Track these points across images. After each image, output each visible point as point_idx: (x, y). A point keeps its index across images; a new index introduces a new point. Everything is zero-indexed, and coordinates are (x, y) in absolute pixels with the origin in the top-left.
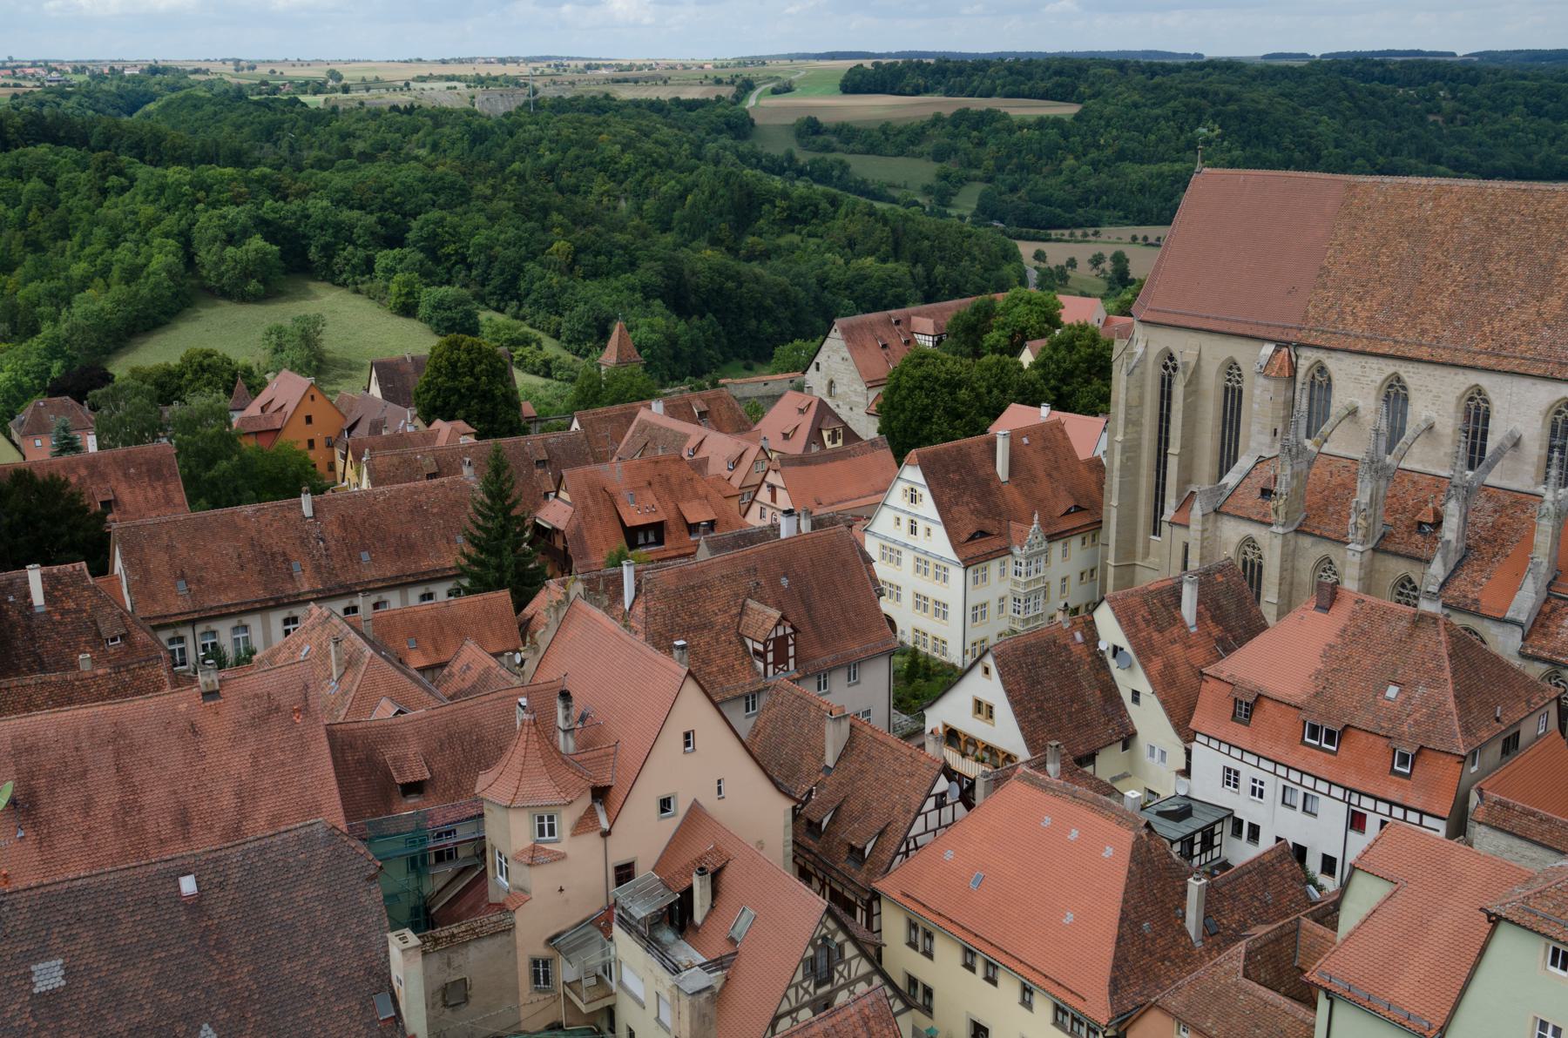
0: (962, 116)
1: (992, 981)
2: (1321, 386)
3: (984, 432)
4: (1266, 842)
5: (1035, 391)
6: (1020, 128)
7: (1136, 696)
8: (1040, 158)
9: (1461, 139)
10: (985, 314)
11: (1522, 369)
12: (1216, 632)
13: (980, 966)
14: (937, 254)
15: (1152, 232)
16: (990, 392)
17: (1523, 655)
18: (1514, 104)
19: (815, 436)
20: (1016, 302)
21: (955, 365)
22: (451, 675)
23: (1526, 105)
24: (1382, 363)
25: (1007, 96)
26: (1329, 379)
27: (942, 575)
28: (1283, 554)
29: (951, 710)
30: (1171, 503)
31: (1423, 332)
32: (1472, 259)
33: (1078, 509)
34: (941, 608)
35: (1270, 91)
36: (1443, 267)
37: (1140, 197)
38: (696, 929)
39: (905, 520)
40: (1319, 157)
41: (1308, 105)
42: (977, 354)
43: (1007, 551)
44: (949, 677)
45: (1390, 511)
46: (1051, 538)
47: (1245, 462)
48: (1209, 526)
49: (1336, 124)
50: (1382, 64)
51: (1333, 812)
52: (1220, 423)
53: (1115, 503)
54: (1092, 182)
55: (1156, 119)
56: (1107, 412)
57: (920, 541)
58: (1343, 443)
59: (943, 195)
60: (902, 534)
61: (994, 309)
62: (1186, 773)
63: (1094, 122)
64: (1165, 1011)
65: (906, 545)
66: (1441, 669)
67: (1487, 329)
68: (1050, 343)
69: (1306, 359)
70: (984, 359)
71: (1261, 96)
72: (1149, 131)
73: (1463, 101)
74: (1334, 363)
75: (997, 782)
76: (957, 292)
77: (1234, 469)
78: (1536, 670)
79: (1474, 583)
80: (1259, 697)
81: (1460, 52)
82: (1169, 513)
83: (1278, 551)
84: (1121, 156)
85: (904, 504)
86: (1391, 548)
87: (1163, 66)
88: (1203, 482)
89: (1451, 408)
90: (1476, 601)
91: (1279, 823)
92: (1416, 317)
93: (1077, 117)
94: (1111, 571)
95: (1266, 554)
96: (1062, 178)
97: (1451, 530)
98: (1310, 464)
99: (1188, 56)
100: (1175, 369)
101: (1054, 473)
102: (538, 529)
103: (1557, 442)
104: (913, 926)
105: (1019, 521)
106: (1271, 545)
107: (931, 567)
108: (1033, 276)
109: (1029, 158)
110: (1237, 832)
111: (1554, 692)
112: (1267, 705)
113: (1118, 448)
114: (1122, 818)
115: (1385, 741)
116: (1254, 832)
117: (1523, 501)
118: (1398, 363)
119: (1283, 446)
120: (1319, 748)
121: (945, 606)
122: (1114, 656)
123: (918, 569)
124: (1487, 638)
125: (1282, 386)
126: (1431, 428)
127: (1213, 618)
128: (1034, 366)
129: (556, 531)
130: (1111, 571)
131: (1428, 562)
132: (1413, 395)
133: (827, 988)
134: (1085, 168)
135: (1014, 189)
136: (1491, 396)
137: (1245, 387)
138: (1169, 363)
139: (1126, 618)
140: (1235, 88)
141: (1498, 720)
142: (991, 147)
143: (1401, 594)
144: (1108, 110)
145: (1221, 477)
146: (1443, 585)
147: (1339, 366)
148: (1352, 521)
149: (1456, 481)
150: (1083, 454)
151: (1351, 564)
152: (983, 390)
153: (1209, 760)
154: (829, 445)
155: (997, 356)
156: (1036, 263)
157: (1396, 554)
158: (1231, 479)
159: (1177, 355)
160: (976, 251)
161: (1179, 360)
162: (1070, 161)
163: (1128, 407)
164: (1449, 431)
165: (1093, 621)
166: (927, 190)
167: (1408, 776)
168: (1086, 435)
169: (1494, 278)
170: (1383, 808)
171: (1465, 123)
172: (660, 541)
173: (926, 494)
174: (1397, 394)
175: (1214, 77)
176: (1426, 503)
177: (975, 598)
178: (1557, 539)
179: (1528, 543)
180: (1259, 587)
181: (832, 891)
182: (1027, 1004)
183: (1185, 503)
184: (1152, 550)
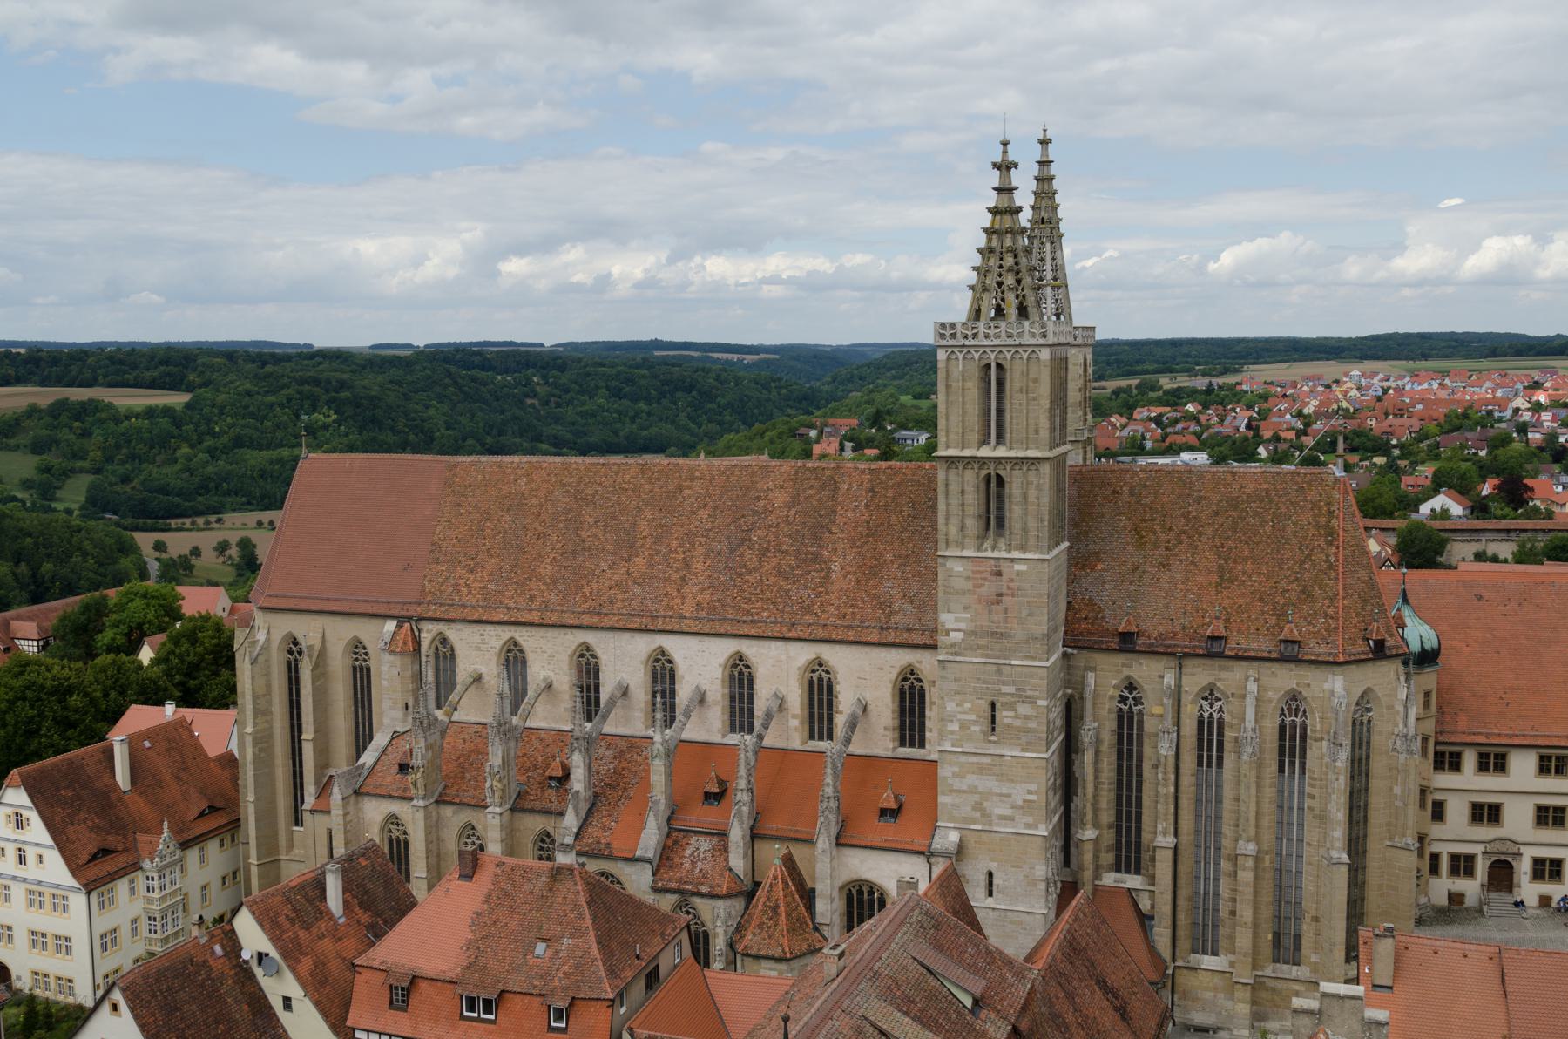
0: (61, 406)
2: (445, 657)
3: (103, 738)
5: (157, 690)
6: (128, 418)
7: (287, 1003)
8: (152, 447)
9: (557, 420)
10: (97, 612)
11: (621, 625)
12: (366, 918)
14: (43, 551)
15: (266, 516)
16: (106, 695)
17: (655, 889)
18: (597, 388)
20: (131, 596)
21: (62, 670)
23: (608, 388)
24: (499, 628)
25: (110, 385)
26: (452, 649)
27: (60, 904)
28: (426, 827)
30: (310, 790)
31: (532, 598)
32: (566, 527)
33: (213, 809)
34: (63, 942)
35: (380, 378)
36: (541, 536)
37: (261, 482)
39: (11, 850)
40: (432, 439)
41: (417, 391)
42: (91, 655)
43: (136, 867)
45: (523, 770)
46: (185, 845)
47: (380, 739)
48: (351, 808)
49: (445, 408)
50: (479, 353)
52: (352, 702)
53: (251, 798)
54: (210, 469)
55: (271, 406)
56: (235, 703)
57: (31, 871)
58: (472, 710)
59: (46, 488)
61: (106, 606)
63: (207, 410)
65: (14, 878)
66: (581, 917)
67: (587, 590)
68: (170, 638)
69: (428, 632)
70: (98, 661)
71: (371, 383)
72: (265, 417)
73: (554, 385)
74: (455, 634)
76: (69, 590)
77: (370, 748)
78: (667, 902)
79: (604, 828)
80: (414, 979)
81: (548, 343)
82: (310, 800)
83: (422, 824)
84: (238, 442)
86: (527, 805)
87: (273, 355)
88: (340, 766)
89: (565, 667)
90: (608, 845)
92: (524, 584)
93: (188, 406)
94: (254, 870)
95: (410, 830)
96: (178, 467)
97: (578, 782)
98: (443, 734)
99: (298, 346)
100: (300, 653)
101: (182, 775)
103: (659, 688)
105: (147, 831)
106: (414, 818)
107: (47, 899)
108: (154, 567)
109: (141, 448)
111: (684, 918)
112: (423, 985)
113: (249, 739)
115: (539, 999)
117: (635, 744)
118: (513, 628)
119: (415, 719)
120: (479, 1020)
121: (67, 939)
122: (260, 963)
123: (31, 903)
124: (622, 879)
125: (408, 660)
126: (549, 686)
127: (361, 905)
128: (154, 662)
130: (254, 870)
131: (561, 814)
132: (530, 657)
134: (201, 455)
135: (125, 480)
136: (599, 652)
137: (372, 664)
138: (293, 647)
139: (267, 921)
140: (345, 376)
141: (638, 957)
142: (97, 437)
143: (541, 849)
144: (221, 398)
145: (358, 757)
146: (577, 835)
147: (459, 636)
148: (488, 785)
149: (577, 734)
150: (213, 750)
151: (491, 824)
152: (98, 694)
155: (113, 655)
156: (157, 554)
157: (532, 811)
158: (368, 758)
159: (300, 639)
160: (87, 545)
161: (304, 644)
162: (185, 449)
163: (255, 697)
164: (566, 687)
165: (233, 930)
166: (27, 484)
167: (564, 1031)
168: (215, 730)
169: (587, 544)
171: (558, 405)
173: (34, 817)
174: (516, 657)
175: (325, 366)
176: (554, 757)
177: (103, 924)
178: (670, 775)
179: (646, 785)
180: (407, 864)
183: (324, 790)
184: (296, 843)
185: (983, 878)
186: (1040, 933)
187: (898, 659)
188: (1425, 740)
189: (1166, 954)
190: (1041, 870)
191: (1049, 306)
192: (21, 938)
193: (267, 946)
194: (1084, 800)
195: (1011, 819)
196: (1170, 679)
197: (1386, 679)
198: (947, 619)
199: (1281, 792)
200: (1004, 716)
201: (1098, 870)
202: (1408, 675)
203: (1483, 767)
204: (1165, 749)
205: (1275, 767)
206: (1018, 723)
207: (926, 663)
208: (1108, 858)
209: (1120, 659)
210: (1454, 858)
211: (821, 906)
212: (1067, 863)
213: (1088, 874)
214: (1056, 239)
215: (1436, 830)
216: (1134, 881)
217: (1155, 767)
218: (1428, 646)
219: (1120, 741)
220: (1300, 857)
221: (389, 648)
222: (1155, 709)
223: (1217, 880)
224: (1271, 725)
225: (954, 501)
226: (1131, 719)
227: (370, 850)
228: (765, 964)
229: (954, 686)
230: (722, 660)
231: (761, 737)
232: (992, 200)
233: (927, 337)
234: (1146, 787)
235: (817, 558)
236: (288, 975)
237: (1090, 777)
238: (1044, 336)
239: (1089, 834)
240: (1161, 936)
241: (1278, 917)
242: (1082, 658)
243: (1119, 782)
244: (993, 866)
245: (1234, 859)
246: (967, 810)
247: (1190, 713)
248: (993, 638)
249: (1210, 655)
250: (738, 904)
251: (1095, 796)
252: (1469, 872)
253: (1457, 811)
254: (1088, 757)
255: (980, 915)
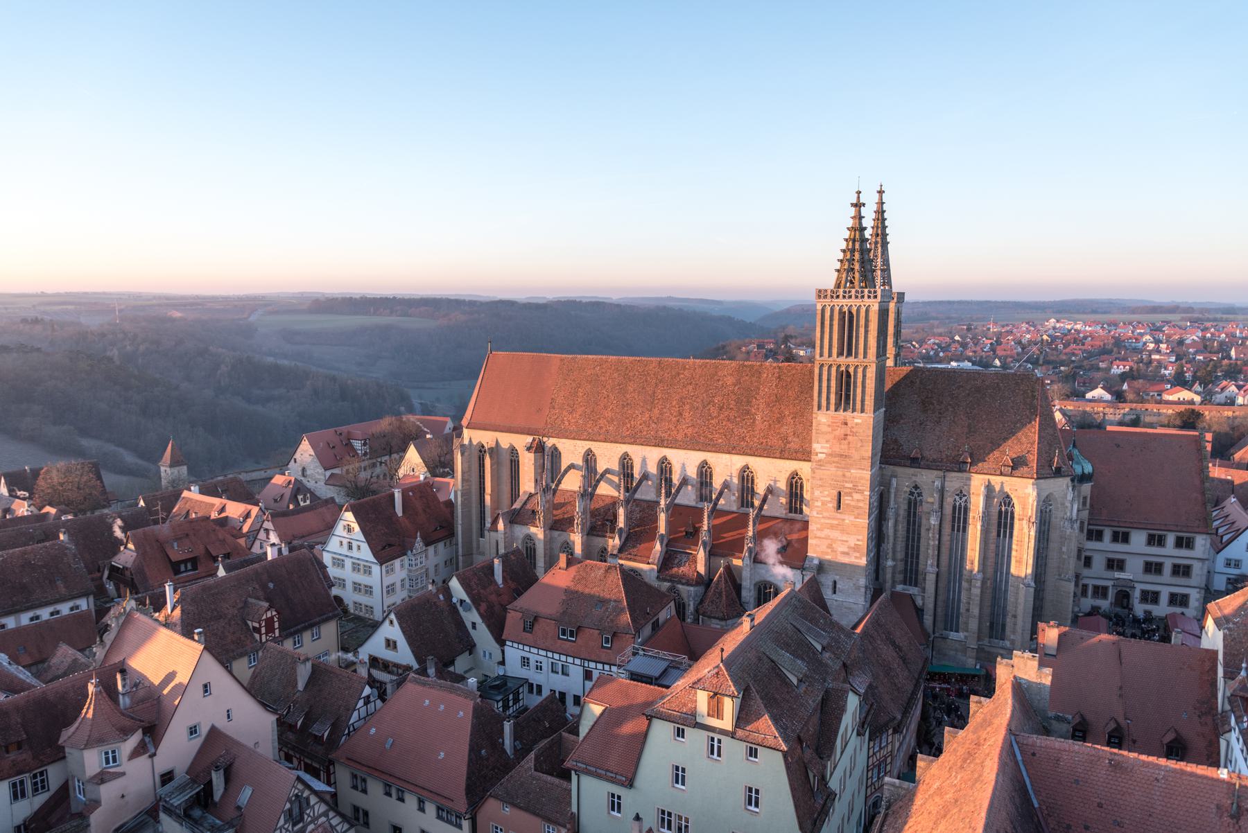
1: (401, 800)
4: (546, 693)
12: (513, 585)
13: (394, 792)
19: (294, 498)
22: (50, 667)
27: (368, 571)
29: (374, 646)
30: (488, 520)
38: (215, 804)
39: (345, 542)
44: (376, 626)
46: (427, 544)
51: (576, 671)
57: (355, 553)
60: (344, 550)
62: (503, 663)
64: (496, 797)
75: (399, 684)
82: (488, 525)
85: (345, 534)
91: (551, 682)
97: (621, 522)
102: (114, 569)
104: (354, 776)
110: (531, 691)
112: (541, 620)
114: (468, 694)
116: (539, 687)
123: (354, 569)
129: (125, 568)
130: (461, 558)
133: (301, 825)
153: (514, 653)
154: (302, 504)
158: (517, 505)
170: (600, 666)
172: (195, 568)
177: (388, 581)
181: (306, 764)
182: (422, 809)
183: (495, 522)
185: (831, 584)
186: (861, 614)
187: (789, 466)
188: (1082, 523)
189: (930, 630)
190: (862, 582)
191: (879, 281)
192: (349, 586)
193: (465, 597)
194: (888, 546)
195: (847, 554)
196: (938, 483)
197: (1061, 486)
198: (816, 447)
199: (998, 547)
200: (845, 500)
201: (894, 583)
202: (1074, 487)
203: (1115, 538)
204: (934, 521)
205: (994, 534)
206: (853, 503)
207: (804, 468)
208: (900, 577)
209: (912, 470)
210: (1096, 588)
211: (744, 593)
212: (877, 578)
213: (888, 585)
214: (885, 244)
215: (1086, 572)
216: (913, 590)
217: (928, 530)
218: (1086, 471)
219: (909, 513)
220: (1007, 582)
221: (529, 449)
222: (930, 499)
223: (960, 592)
224: (994, 511)
225: (825, 384)
226: (915, 504)
227: (518, 549)
228: (714, 621)
229: (819, 483)
230: (697, 463)
231: (716, 504)
232: (850, 223)
233: (812, 297)
234: (922, 540)
235: (748, 412)
236: (474, 611)
237: (891, 532)
238: (875, 297)
239: (890, 563)
240: (928, 619)
241: (992, 614)
242: (890, 469)
243: (908, 537)
244: (837, 578)
245: (970, 581)
246: (824, 548)
247: (949, 501)
248: (842, 458)
249: (960, 471)
250: (701, 589)
251: (894, 544)
252: (1105, 596)
253: (1099, 562)
254: (891, 523)
255: (829, 603)
